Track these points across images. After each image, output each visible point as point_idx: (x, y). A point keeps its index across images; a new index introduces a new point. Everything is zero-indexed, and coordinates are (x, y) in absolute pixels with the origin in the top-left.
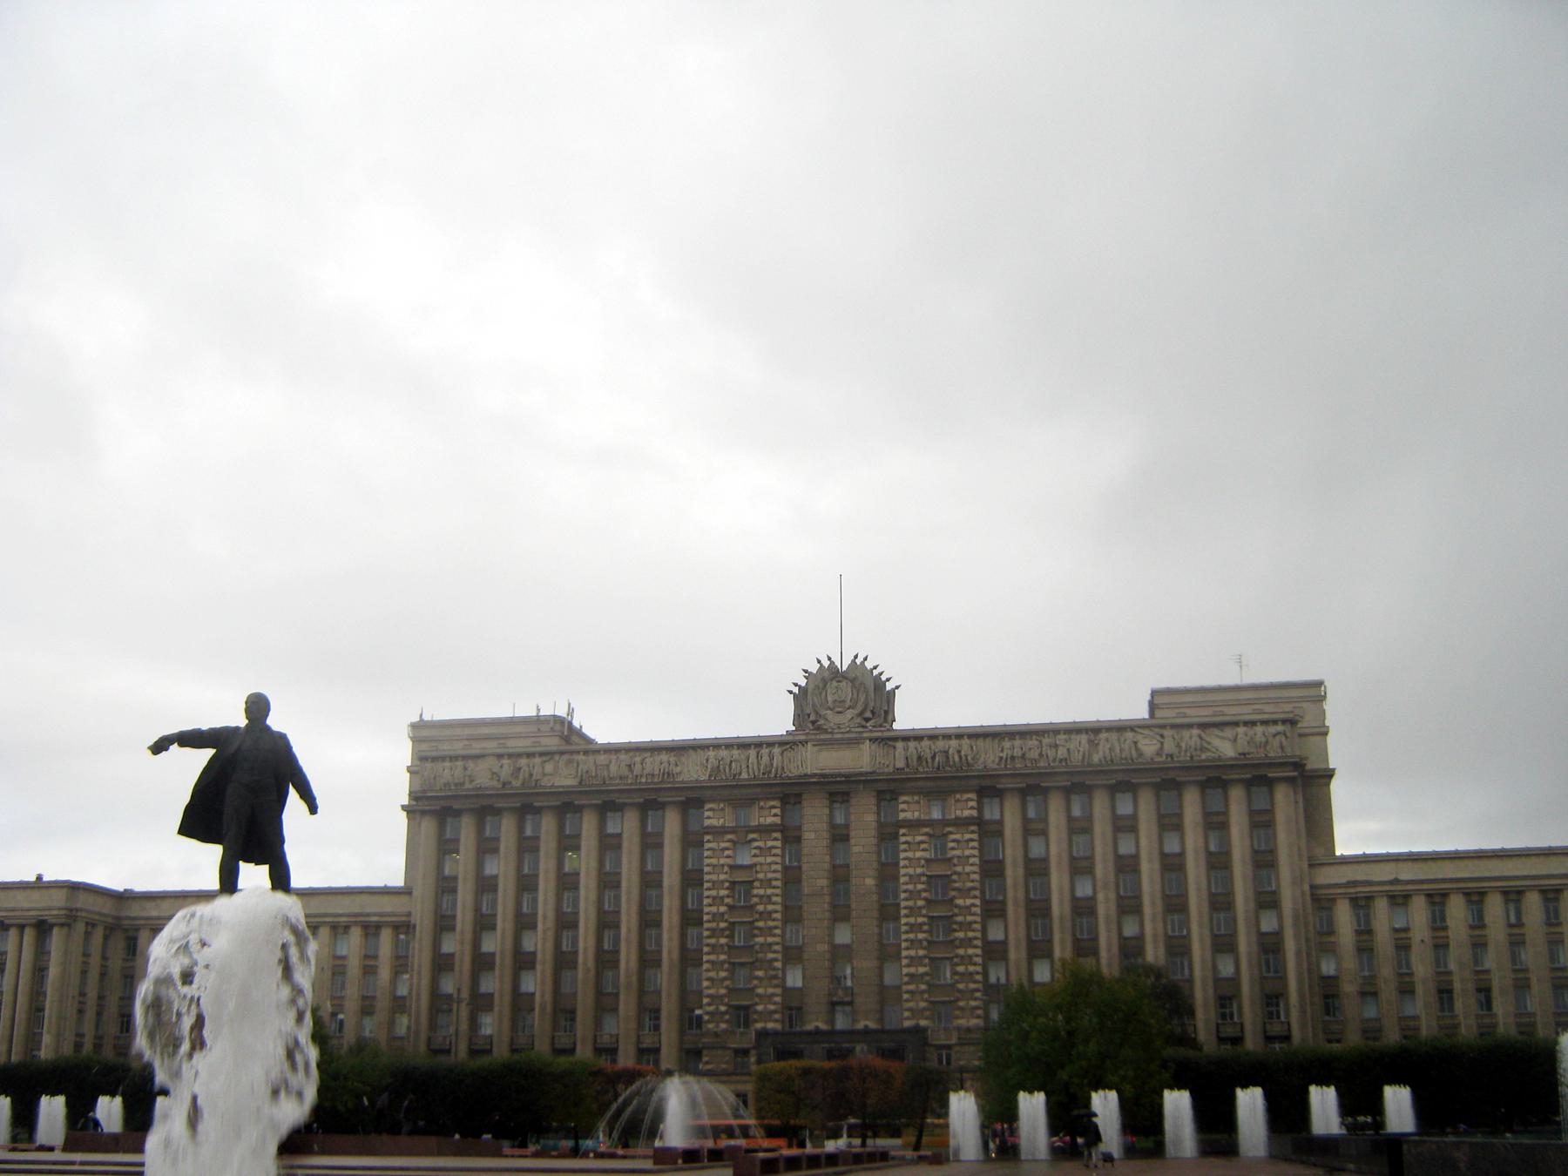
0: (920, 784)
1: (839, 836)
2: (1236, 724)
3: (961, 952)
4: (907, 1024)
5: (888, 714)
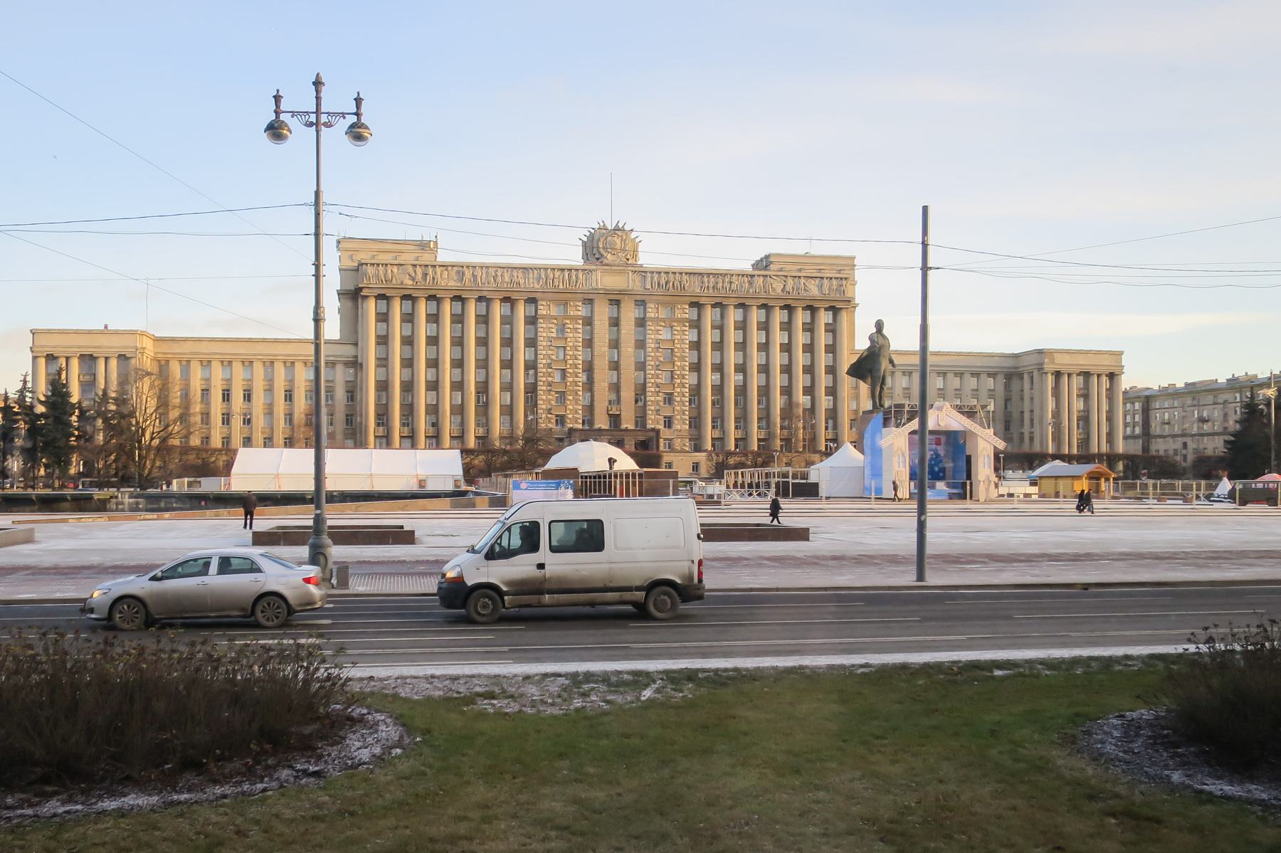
1: (615, 323)
4: (649, 426)
5: (635, 256)
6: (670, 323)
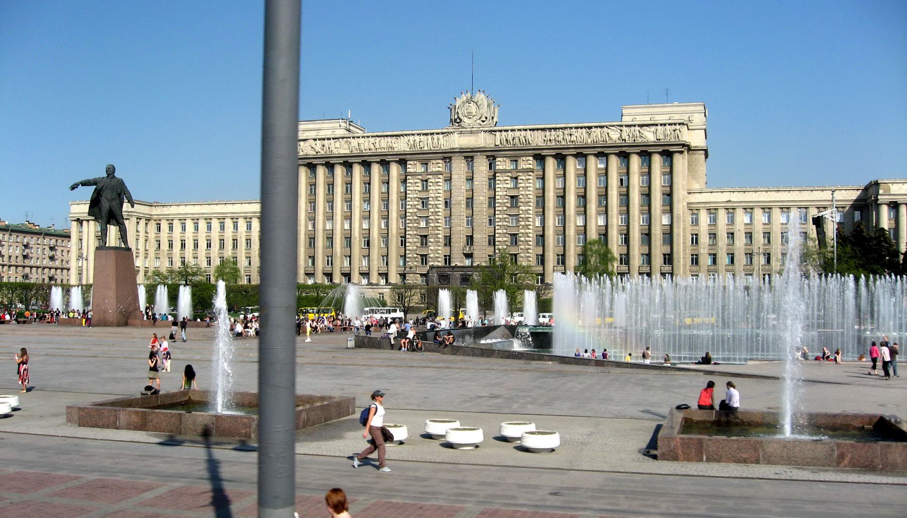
2: (657, 125)
3: (523, 231)
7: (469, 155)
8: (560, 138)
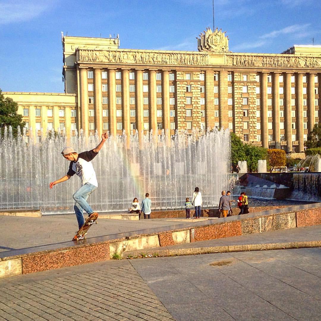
0: (241, 70)
6: (246, 84)
7: (218, 70)
8: (272, 62)
